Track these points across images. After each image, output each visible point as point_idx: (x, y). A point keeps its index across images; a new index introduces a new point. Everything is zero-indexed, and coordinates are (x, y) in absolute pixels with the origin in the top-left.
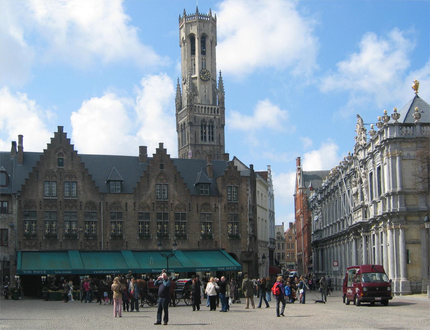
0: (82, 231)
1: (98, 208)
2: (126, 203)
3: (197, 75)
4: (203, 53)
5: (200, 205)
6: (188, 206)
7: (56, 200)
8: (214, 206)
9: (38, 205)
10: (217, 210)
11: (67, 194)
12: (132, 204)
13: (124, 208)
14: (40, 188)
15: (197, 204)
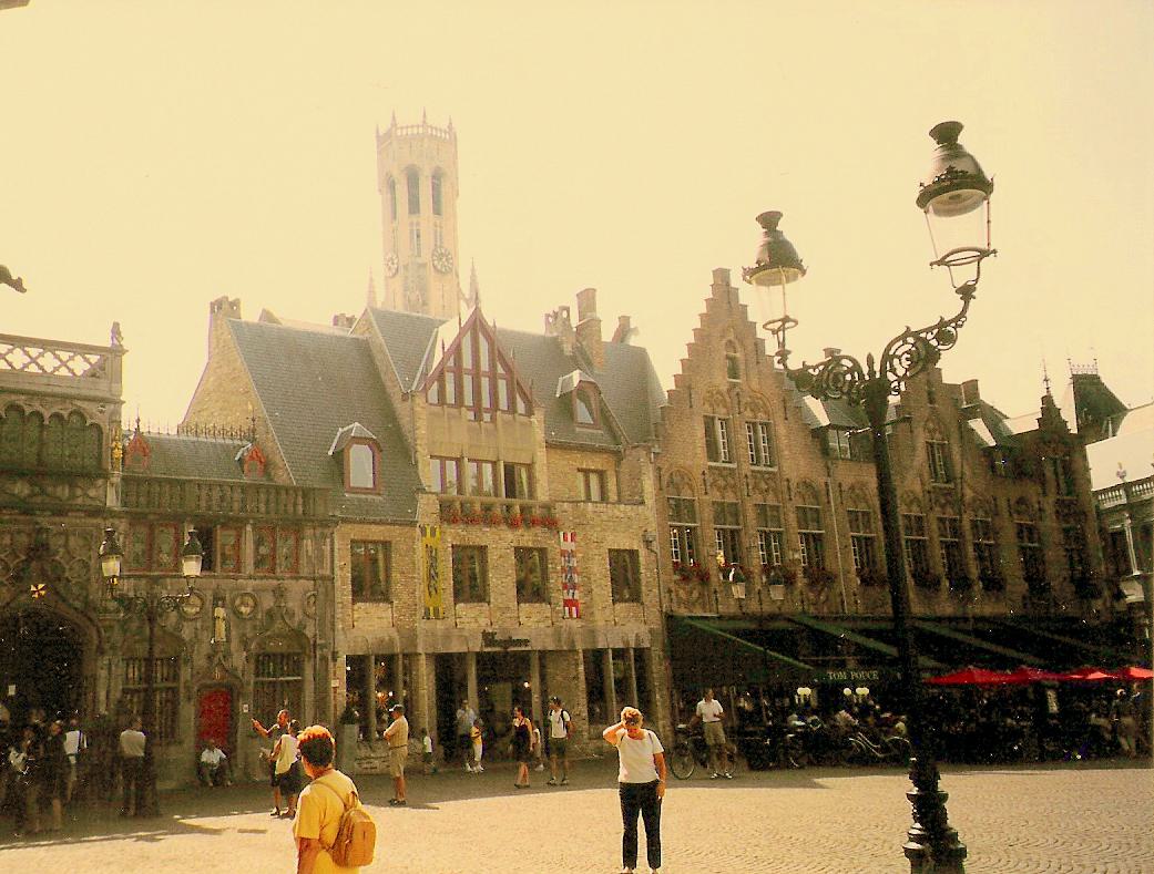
1: (824, 499)
3: (426, 257)
4: (437, 211)
5: (1012, 502)
7: (733, 470)
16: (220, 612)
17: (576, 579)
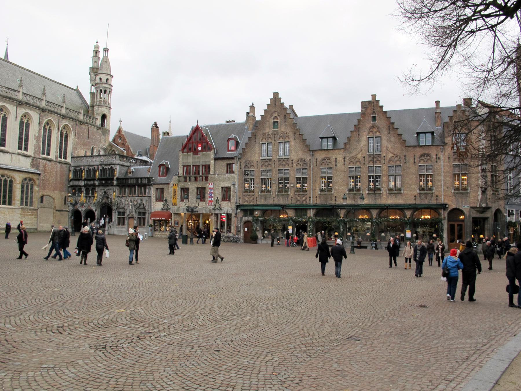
0: (293, 187)
1: (309, 165)
2: (336, 159)
6: (404, 158)
8: (435, 157)
9: (255, 165)
10: (438, 161)
11: (281, 153)
12: (342, 159)
13: (334, 163)
14: (257, 150)
15: (415, 156)
16: (131, 204)
17: (213, 195)
